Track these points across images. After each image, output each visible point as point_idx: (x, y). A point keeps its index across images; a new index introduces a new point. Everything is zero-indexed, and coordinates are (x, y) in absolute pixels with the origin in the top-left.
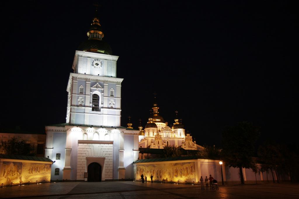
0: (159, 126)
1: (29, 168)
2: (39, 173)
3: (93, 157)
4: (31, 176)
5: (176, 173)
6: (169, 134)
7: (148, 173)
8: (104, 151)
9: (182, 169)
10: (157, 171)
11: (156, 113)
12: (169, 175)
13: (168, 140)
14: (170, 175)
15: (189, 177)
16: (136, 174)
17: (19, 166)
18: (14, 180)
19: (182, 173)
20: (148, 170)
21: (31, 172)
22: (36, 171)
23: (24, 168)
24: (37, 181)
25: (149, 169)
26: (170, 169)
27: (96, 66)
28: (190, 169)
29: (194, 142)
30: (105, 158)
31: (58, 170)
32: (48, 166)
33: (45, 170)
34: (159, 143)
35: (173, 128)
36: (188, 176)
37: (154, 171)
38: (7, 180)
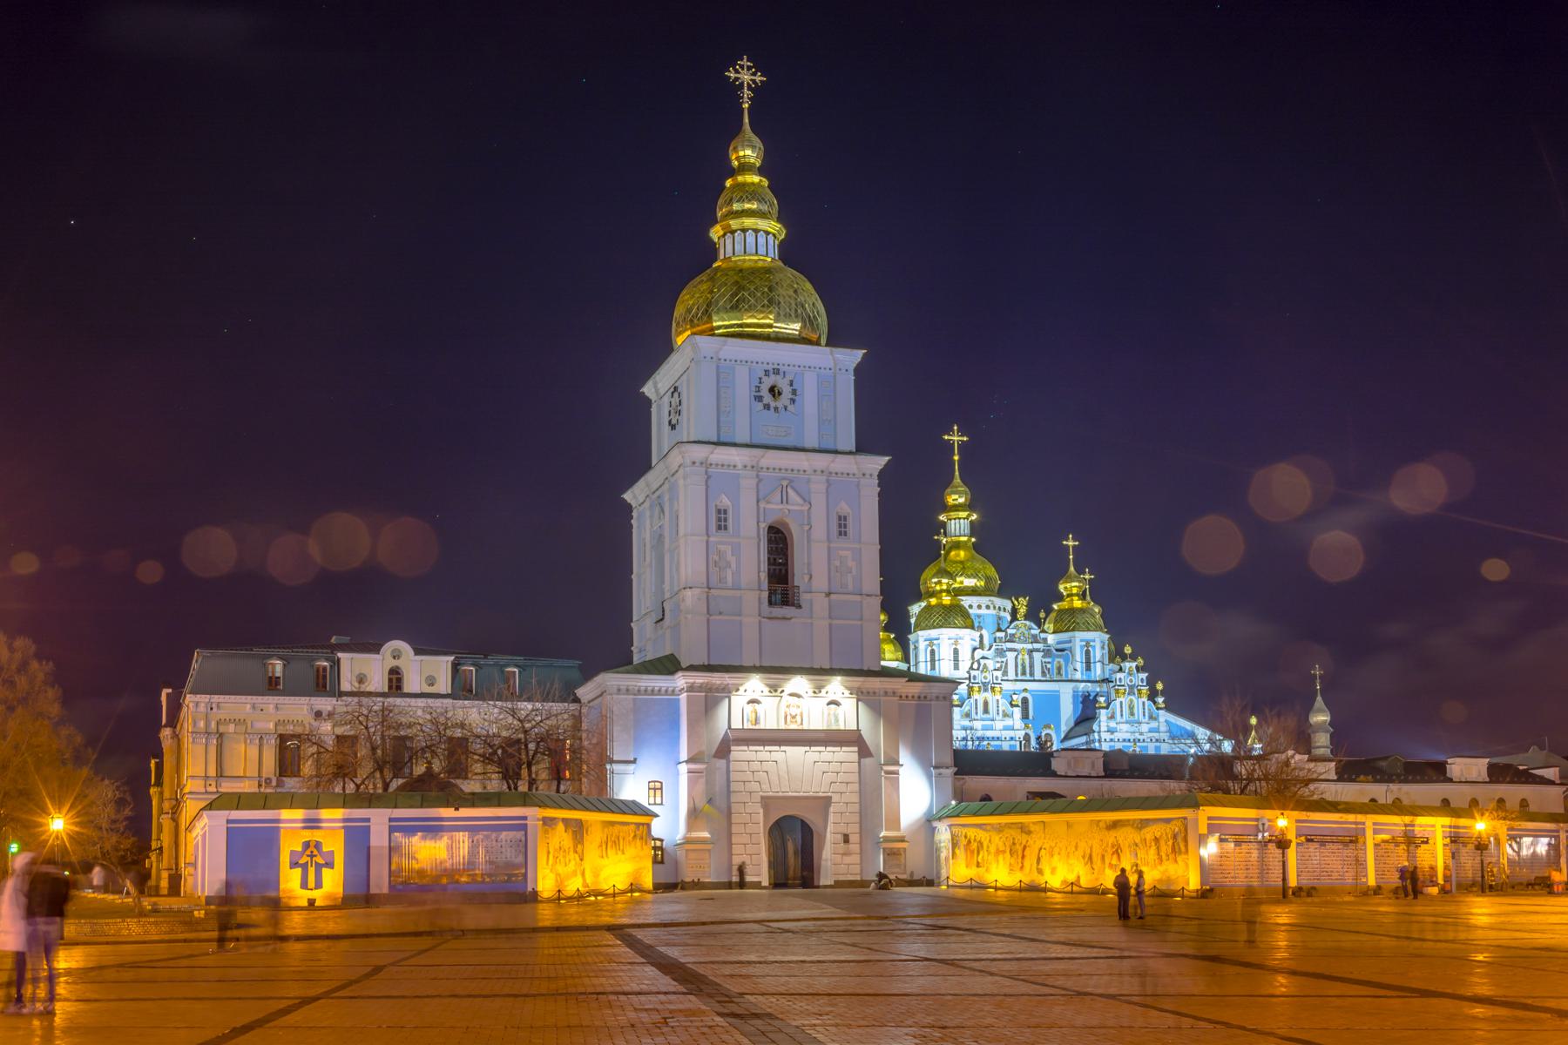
0: (979, 616)
3: (777, 794)
5: (1115, 857)
6: (1031, 658)
7: (1001, 858)
8: (825, 767)
9: (1137, 841)
10: (1041, 849)
11: (957, 546)
12: (1086, 864)
13: (1025, 690)
14: (1092, 863)
16: (947, 859)
19: (1136, 855)
20: (1001, 844)
26: (1090, 842)
27: (768, 398)
28: (1170, 843)
29: (1155, 703)
30: (830, 798)
34: (986, 711)
35: (1049, 626)
36: (1159, 867)
37: (1028, 848)
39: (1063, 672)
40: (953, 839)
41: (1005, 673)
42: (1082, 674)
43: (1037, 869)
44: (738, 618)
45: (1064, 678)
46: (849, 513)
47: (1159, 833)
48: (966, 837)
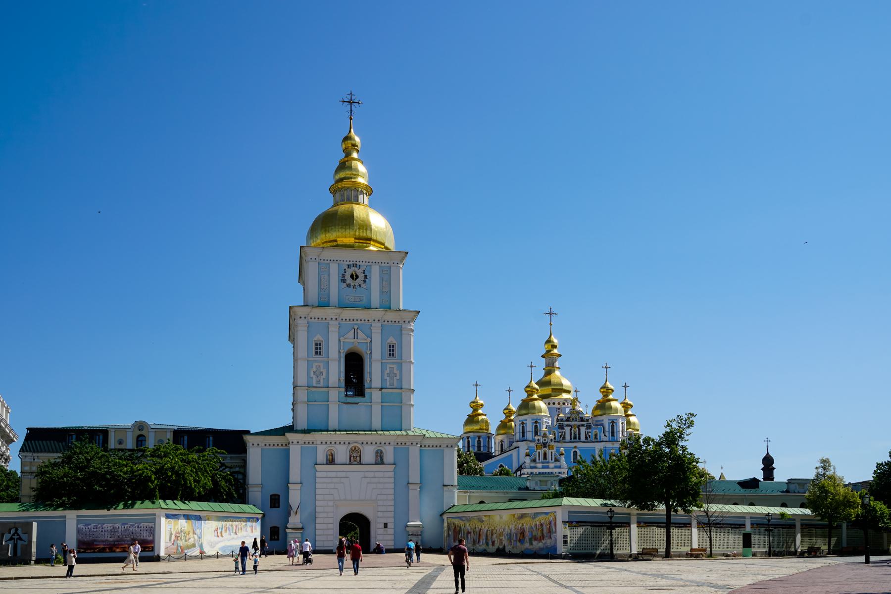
1: (214, 529)
2: (236, 536)
4: (220, 542)
5: (522, 535)
10: (487, 531)
12: (508, 539)
13: (575, 447)
15: (544, 544)
18: (188, 549)
20: (469, 528)
21: (219, 535)
23: (206, 526)
25: (471, 525)
26: (510, 527)
33: (247, 531)
36: (542, 541)
38: (177, 549)
39: (598, 437)
40: (448, 525)
41: (564, 438)
42: (609, 438)
43: (486, 542)
44: (326, 403)
45: (598, 440)
46: (395, 343)
47: (543, 521)
48: (454, 524)
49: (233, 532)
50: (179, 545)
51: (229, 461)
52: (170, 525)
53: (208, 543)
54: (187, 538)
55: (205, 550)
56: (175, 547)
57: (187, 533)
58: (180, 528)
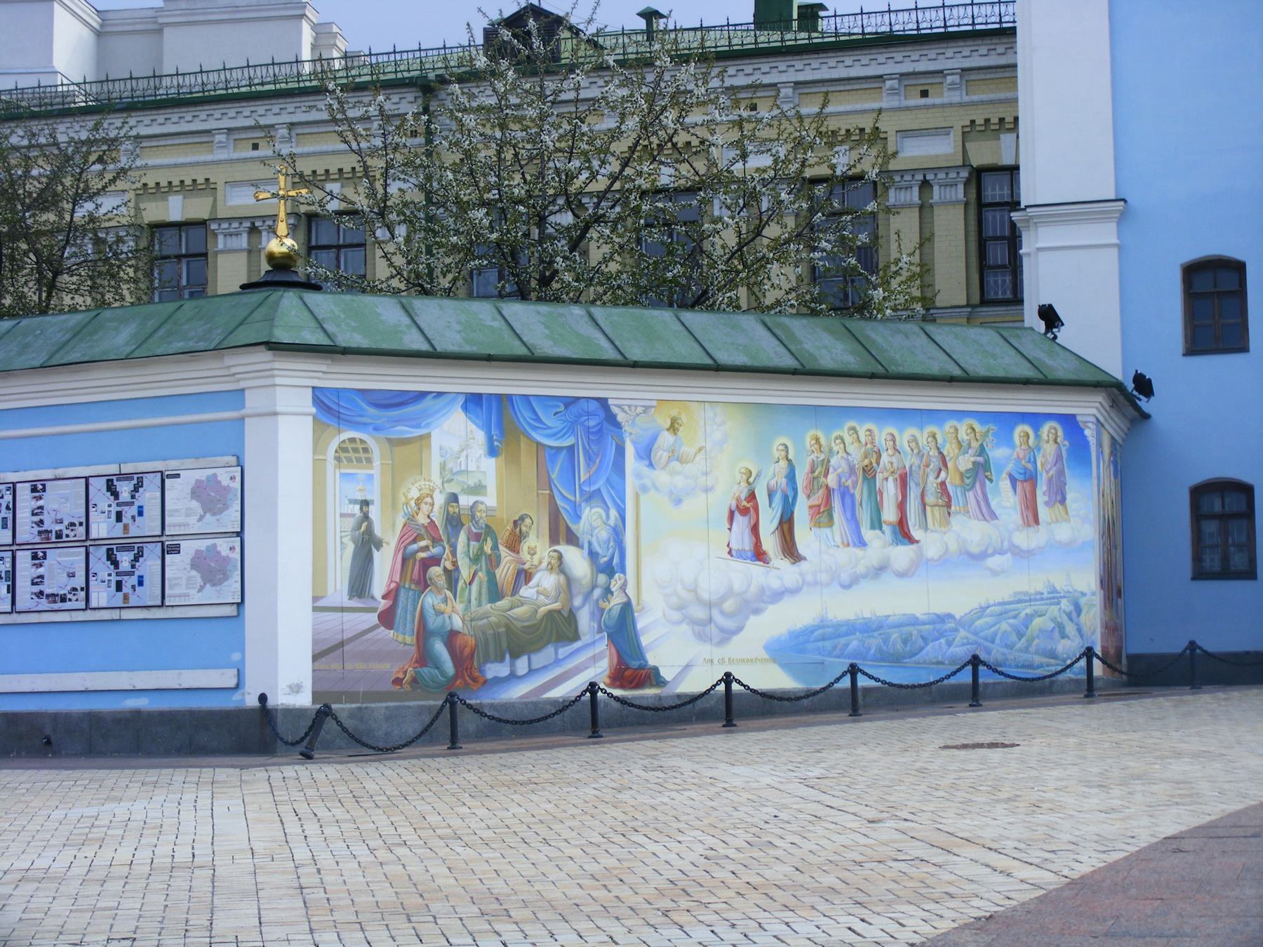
1: (727, 491)
2: (902, 555)
4: (777, 596)
17: (571, 449)
18: (515, 656)
21: (770, 542)
22: (854, 521)
23: (661, 477)
24: (853, 671)
31: (1234, 503)
32: (1032, 452)
38: (424, 657)
49: (877, 523)
50: (433, 622)
51: (955, 97)
52: (362, 472)
53: (680, 608)
54: (505, 572)
55: (652, 660)
56: (402, 638)
57: (504, 533)
58: (439, 499)
